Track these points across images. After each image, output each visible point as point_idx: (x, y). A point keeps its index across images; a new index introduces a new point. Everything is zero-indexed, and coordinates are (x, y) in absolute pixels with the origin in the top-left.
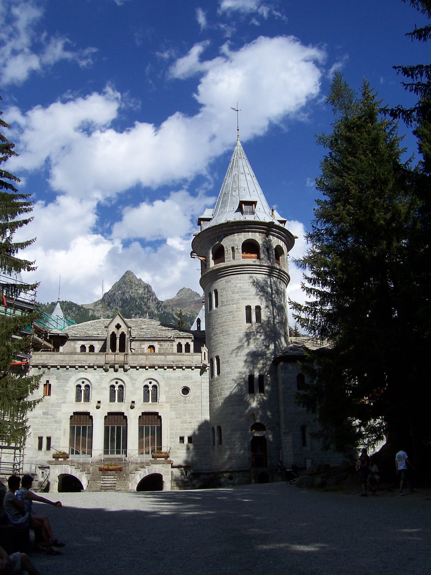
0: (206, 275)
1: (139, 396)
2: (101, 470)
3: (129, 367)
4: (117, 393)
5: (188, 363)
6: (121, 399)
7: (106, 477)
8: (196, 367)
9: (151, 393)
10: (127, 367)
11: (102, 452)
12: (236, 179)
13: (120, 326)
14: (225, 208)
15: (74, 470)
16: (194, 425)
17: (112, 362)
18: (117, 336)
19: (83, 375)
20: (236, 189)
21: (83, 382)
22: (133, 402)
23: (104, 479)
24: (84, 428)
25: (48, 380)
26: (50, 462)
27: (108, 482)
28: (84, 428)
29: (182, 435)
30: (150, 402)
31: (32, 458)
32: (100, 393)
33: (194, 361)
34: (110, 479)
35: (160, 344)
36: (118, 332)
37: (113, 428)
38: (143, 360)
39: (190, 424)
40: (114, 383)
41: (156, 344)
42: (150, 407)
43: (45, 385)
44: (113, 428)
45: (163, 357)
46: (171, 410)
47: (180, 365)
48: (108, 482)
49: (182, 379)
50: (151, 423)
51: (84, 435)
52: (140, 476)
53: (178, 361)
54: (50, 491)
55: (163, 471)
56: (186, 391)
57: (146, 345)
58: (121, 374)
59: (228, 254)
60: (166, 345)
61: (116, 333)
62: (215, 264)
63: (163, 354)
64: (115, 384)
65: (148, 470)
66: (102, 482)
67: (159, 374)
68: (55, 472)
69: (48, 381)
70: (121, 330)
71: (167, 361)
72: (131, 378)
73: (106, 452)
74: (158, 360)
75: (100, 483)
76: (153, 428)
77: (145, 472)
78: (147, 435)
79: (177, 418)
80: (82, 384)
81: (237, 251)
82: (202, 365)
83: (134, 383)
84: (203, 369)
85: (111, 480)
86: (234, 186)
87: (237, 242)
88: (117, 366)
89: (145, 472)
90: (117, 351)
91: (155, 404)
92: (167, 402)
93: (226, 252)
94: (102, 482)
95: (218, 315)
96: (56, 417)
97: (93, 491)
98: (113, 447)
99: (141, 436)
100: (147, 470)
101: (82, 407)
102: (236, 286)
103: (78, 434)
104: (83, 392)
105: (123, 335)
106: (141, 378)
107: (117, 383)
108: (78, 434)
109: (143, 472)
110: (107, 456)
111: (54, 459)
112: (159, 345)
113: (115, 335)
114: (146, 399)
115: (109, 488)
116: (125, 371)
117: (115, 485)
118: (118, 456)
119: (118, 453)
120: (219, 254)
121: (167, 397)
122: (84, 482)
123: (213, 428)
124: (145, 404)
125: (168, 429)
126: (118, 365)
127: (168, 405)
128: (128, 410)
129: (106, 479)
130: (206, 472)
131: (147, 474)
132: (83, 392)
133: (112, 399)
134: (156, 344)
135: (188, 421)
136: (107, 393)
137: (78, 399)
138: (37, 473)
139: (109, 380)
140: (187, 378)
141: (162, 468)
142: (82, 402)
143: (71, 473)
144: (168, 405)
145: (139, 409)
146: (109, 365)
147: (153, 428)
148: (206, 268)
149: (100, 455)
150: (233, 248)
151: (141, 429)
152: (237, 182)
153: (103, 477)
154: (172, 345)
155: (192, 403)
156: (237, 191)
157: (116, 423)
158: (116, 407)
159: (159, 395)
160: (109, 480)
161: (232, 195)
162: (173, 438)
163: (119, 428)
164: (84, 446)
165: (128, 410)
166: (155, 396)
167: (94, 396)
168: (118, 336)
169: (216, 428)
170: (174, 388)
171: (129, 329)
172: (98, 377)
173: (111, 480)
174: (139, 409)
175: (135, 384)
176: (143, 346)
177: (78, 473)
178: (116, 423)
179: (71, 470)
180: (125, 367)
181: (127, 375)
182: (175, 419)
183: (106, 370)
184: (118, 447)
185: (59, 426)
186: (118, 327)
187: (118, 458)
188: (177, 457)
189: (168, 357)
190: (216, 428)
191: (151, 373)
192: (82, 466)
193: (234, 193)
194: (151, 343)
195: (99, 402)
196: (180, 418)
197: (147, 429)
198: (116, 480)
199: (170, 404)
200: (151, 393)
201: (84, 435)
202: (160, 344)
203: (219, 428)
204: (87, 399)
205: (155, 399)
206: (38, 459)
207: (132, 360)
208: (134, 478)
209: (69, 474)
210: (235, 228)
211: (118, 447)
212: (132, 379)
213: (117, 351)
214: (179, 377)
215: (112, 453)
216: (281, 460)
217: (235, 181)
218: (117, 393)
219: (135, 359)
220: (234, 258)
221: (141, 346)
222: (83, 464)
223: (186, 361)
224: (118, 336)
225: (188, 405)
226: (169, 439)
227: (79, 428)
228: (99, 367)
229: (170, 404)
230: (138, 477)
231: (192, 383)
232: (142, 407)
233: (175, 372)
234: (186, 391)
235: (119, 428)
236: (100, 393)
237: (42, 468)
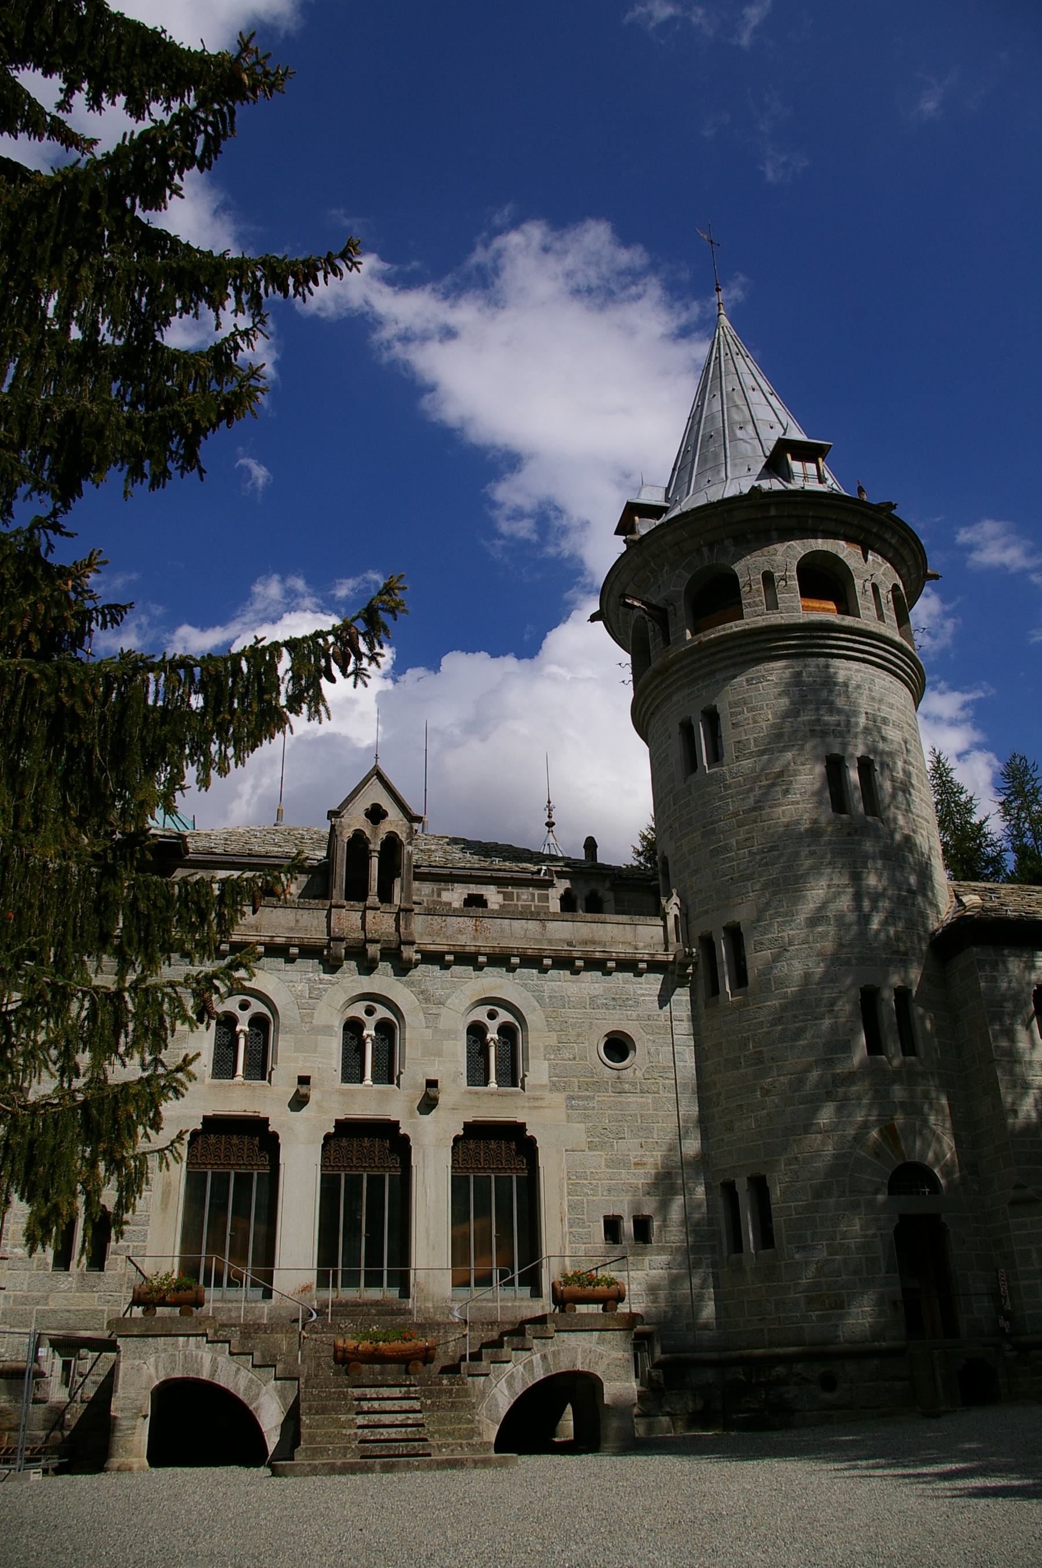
0: (663, 671)
1: (452, 1062)
2: (344, 1359)
3: (419, 956)
4: (372, 1047)
5: (621, 950)
6: (387, 1073)
7: (370, 1392)
8: (654, 966)
9: (496, 1050)
10: (409, 953)
11: (312, 1277)
12: (740, 402)
14: (719, 471)
15: (223, 1359)
17: (355, 935)
18: (371, 847)
20: (745, 422)
22: (432, 1084)
23: (366, 1405)
24: (243, 1181)
26: (120, 1326)
27: (386, 1419)
28: (243, 1181)
30: (493, 1085)
31: (25, 1300)
32: (312, 1046)
33: (641, 945)
34: (390, 1405)
35: (504, 893)
36: (375, 834)
37: (354, 1183)
38: (463, 933)
40: (358, 1010)
41: (493, 896)
42: (495, 1105)
44: (354, 1183)
45: (533, 926)
47: (598, 955)
48: (386, 1419)
50: (499, 1164)
51: (241, 1210)
52: (510, 1385)
53: (585, 943)
54: (115, 1462)
55: (606, 1361)
56: (618, 1046)
57: (455, 895)
58: (382, 980)
59: (753, 596)
60: (525, 896)
61: (368, 833)
62: (692, 635)
64: (363, 1016)
65: (544, 1357)
66: (361, 1420)
67: (524, 986)
68: (139, 1369)
70: (385, 827)
71: (550, 941)
72: (425, 997)
73: (323, 1281)
74: (518, 934)
75: (352, 1426)
76: (504, 1185)
77: (529, 1366)
78: (482, 1211)
80: (239, 1013)
81: (783, 583)
82: (671, 958)
83: (438, 1015)
84: (672, 974)
85: (396, 1405)
86: (737, 417)
87: (779, 558)
88: (373, 950)
89: (529, 1366)
90: (373, 899)
91: (511, 1094)
92: (554, 1087)
93: (747, 588)
94: (361, 1420)
95: (727, 787)
97: (333, 1470)
98: (352, 1259)
99: (459, 1216)
100: (536, 1358)
103: (219, 1208)
105: (392, 843)
106: (461, 994)
107: (370, 1012)
108: (219, 1208)
109: (521, 1368)
110: (329, 1295)
111: (138, 1311)
112: (501, 896)
113: (367, 842)
114: (477, 1075)
115: (402, 1448)
116: (402, 968)
117: (423, 1433)
118: (374, 1294)
119: (374, 1280)
120: (719, 596)
121: (553, 1067)
122: (270, 1418)
124: (476, 1093)
125: (562, 1191)
126: (379, 946)
127: (559, 1098)
128: (411, 1115)
129: (376, 1405)
130: (714, 1355)
131: (540, 1375)
133: (352, 1072)
134: (493, 896)
135: (633, 1160)
136: (335, 1045)
138: (45, 1367)
139: (343, 998)
140: (620, 1001)
141: (600, 1349)
142: (239, 1079)
143: (213, 1375)
144: (558, 1098)
146: (344, 945)
147: (504, 1185)
148: (667, 642)
149: (306, 1289)
150: (768, 578)
151: (459, 1186)
152: (745, 408)
153: (357, 1392)
154: (546, 898)
155: (642, 1092)
156: (750, 428)
157: (367, 1161)
158: (368, 1101)
159: (526, 1059)
160: (388, 1405)
161: (734, 439)
162: (581, 1223)
163: (376, 1183)
164: (239, 1254)
166: (508, 1063)
167: (288, 1059)
168: (376, 846)
169: (742, 1186)
170: (579, 1035)
171: (416, 826)
172: (302, 987)
173: (396, 1405)
176: (446, 896)
177: (243, 1372)
178: (367, 1161)
179: (214, 1361)
180: (405, 955)
181: (410, 984)
182: (587, 1152)
183: (332, 966)
184: (374, 1258)
186: (376, 814)
187: (376, 1303)
189: (550, 925)
190: (742, 1186)
191: (494, 982)
192: (246, 1340)
193: (739, 434)
194: (475, 889)
195: (304, 1080)
197: (482, 1186)
198: (417, 1405)
199: (563, 1095)
200: (496, 1050)
201: (241, 1210)
202: (504, 893)
204: (260, 1068)
205: (511, 1076)
206: (52, 1305)
207: (423, 931)
208: (483, 1394)
209: (205, 1376)
210: (773, 512)
211: (374, 1258)
212: (427, 1000)
213: (373, 899)
214: (593, 998)
215: (351, 1281)
216: (1008, 1307)
217: (737, 406)
218: (372, 1047)
219: (436, 927)
220: (773, 605)
221: (439, 895)
222: (250, 1330)
223: (614, 942)
224: (376, 846)
225: (632, 1098)
226: (566, 1229)
227: (221, 1181)
228: (309, 951)
229: (563, 1095)
230: (501, 1389)
232: (463, 1104)
233: (577, 981)
234: (618, 1046)
235: (376, 1183)
236: (312, 1046)
237: (67, 1346)
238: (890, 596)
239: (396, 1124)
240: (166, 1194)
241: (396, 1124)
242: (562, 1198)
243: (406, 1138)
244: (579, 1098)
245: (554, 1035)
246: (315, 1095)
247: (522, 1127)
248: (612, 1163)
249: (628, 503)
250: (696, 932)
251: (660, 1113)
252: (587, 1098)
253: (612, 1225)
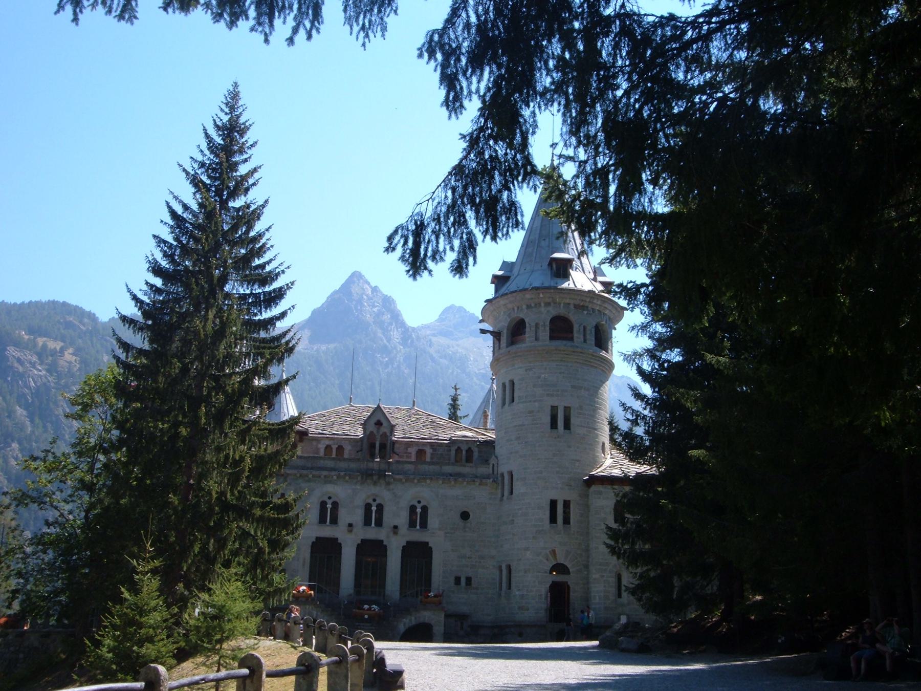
1: (402, 520)
4: (373, 514)
9: (419, 517)
13: (381, 424)
19: (330, 488)
21: (330, 498)
30: (418, 527)
32: (352, 514)
36: (378, 432)
42: (418, 536)
52: (405, 624)
56: (465, 516)
61: (375, 432)
63: (437, 463)
77: (411, 620)
92: (440, 529)
101: (327, 531)
102: (539, 377)
104: (329, 513)
107: (374, 500)
114: (412, 524)
123: (500, 567)
132: (329, 513)
133: (367, 522)
137: (322, 520)
158: (372, 533)
167: (344, 517)
200: (419, 517)
203: (509, 568)
204: (334, 521)
205: (424, 525)
218: (373, 514)
232: (406, 535)
234: (465, 516)
236: (352, 514)
238: (593, 330)
239: (382, 541)
240: (304, 562)
241: (382, 541)
243: (386, 546)
247: (427, 543)
249: (504, 262)
250: (500, 472)
253: (458, 580)
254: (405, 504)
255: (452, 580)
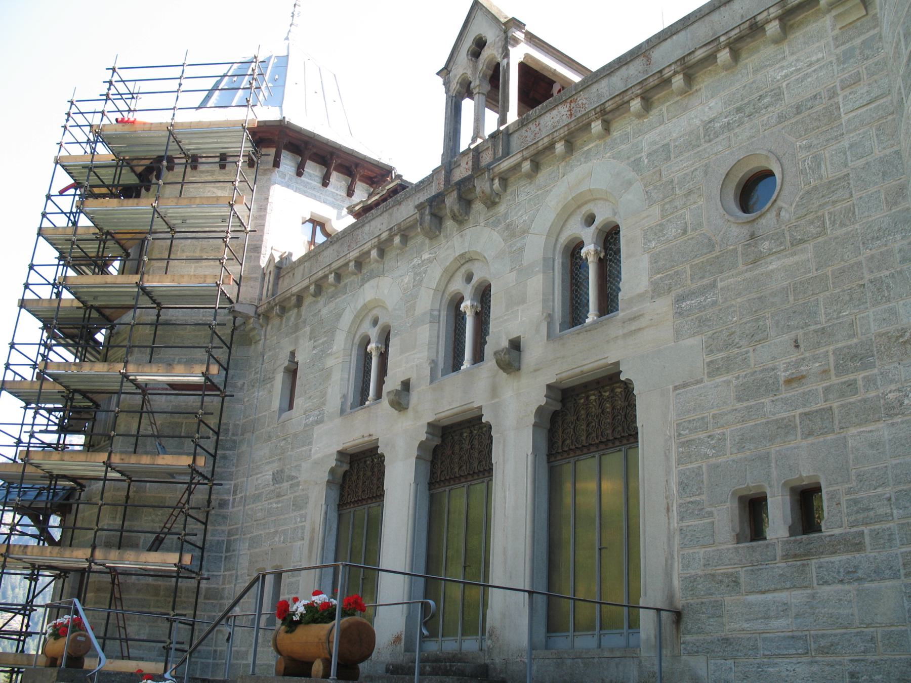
16: (820, 387)
25: (291, 349)
29: (750, 483)
39: (797, 391)
43: (287, 370)
46: (678, 334)
49: (728, 127)
69: (293, 354)
79: (714, 370)
96: (298, 484)
121: (654, 259)
125: (667, 458)
135: (783, 375)
144: (663, 306)
145: (535, 371)
165: (494, 391)
174: (535, 371)
175: (522, 249)
182: (707, 382)
185: (301, 516)
188: (726, 640)
196: (728, 366)
212: (513, 235)
226: (675, 524)
231: (782, 118)
232: (558, 359)
242: (668, 473)
244: (693, 294)
245: (656, 210)
246: (414, 397)
248: (745, 392)
251: (829, 270)
252: (703, 291)
253: (753, 508)
254: (535, 247)
255: (725, 517)
